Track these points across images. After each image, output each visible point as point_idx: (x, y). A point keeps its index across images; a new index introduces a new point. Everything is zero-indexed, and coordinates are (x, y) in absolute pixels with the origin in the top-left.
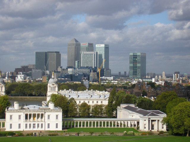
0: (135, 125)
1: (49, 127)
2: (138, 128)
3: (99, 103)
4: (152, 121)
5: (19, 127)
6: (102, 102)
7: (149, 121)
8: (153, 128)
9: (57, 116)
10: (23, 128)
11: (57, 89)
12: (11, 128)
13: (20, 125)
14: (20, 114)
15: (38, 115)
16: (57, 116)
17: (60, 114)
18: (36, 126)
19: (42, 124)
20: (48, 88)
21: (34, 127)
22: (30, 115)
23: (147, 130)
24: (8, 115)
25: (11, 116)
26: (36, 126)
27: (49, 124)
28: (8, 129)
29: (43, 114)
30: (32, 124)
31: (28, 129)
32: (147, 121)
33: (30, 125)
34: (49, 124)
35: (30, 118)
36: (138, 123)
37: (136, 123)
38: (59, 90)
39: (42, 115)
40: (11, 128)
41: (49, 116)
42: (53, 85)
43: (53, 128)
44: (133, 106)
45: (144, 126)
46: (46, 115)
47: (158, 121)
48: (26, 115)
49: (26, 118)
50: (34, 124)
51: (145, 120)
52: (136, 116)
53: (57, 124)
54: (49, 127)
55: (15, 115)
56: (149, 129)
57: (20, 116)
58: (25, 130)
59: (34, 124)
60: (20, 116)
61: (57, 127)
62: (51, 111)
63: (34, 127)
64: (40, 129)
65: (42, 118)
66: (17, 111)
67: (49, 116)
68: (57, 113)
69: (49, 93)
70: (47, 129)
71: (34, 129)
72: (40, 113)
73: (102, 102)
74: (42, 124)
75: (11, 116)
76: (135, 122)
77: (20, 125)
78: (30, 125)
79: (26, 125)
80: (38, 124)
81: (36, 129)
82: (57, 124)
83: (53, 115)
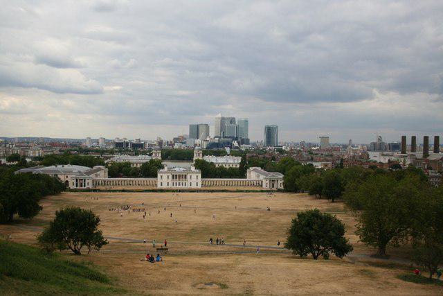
2: (262, 186)
3: (234, 166)
8: (273, 187)
10: (171, 186)
11: (201, 155)
17: (200, 175)
20: (195, 155)
24: (159, 175)
25: (161, 176)
28: (159, 187)
30: (178, 183)
32: (268, 182)
35: (176, 178)
37: (260, 183)
38: (203, 156)
43: (194, 186)
44: (259, 169)
46: (188, 176)
48: (173, 175)
49: (173, 178)
52: (262, 177)
55: (165, 176)
58: (172, 187)
60: (168, 176)
63: (179, 185)
69: (194, 159)
70: (189, 187)
75: (161, 176)
83: (194, 176)
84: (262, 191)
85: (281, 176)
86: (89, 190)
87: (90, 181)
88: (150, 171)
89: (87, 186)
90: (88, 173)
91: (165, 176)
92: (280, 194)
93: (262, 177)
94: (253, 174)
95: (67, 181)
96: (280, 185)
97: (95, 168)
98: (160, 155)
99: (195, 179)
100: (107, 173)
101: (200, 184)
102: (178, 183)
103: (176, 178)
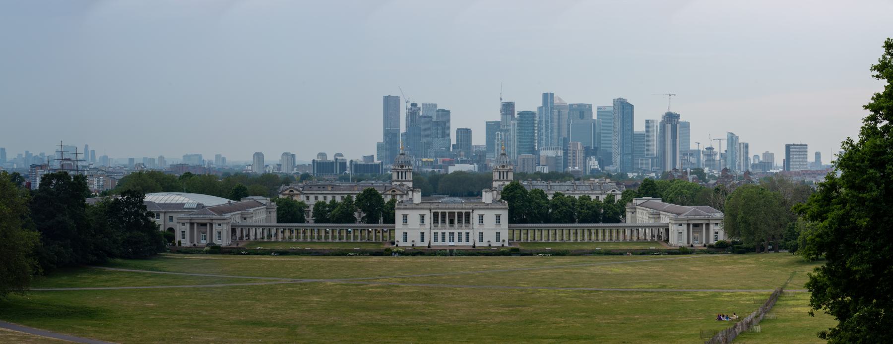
0: (659, 237)
1: (481, 240)
2: (667, 241)
4: (695, 225)
5: (422, 240)
6: (598, 198)
7: (688, 225)
9: (498, 217)
12: (405, 240)
13: (422, 234)
14: (422, 212)
15: (460, 214)
16: (498, 217)
17: (505, 215)
18: (456, 236)
19: (467, 234)
20: (496, 176)
21: (452, 240)
22: (444, 214)
23: (684, 243)
24: (399, 215)
25: (405, 217)
26: (456, 236)
27: (481, 234)
29: (469, 213)
30: (447, 232)
31: (440, 243)
33: (443, 234)
34: (481, 234)
35: (443, 221)
36: (667, 230)
39: (468, 215)
40: (405, 240)
41: (481, 218)
42: (503, 166)
45: (678, 237)
47: (708, 225)
48: (436, 215)
49: (436, 221)
50: (452, 234)
51: (680, 225)
53: (498, 234)
54: (481, 240)
55: (414, 216)
56: (688, 243)
57: (422, 217)
59: (452, 234)
60: (422, 217)
61: (498, 239)
62: (487, 207)
63: (452, 240)
64: (464, 243)
65: (468, 221)
66: (416, 208)
67: (481, 218)
68: (498, 212)
71: (452, 244)
72: (464, 211)
73: (598, 198)
74: (467, 234)
75: (405, 217)
76: (661, 230)
77: (422, 234)
78: (443, 234)
79: (436, 234)
80: (460, 234)
81: (456, 243)
82: (498, 234)
83: (490, 216)
84: (670, 253)
85: (719, 215)
86: (215, 250)
87: (225, 229)
88: (377, 209)
89: (216, 241)
90: (219, 210)
91: (414, 216)
92: (721, 257)
93: (664, 219)
94: (641, 215)
95: (171, 230)
96: (718, 233)
97: (244, 201)
98: (410, 176)
99: (491, 225)
100: (274, 215)
101: (505, 235)
102: (447, 232)
103: (443, 221)
